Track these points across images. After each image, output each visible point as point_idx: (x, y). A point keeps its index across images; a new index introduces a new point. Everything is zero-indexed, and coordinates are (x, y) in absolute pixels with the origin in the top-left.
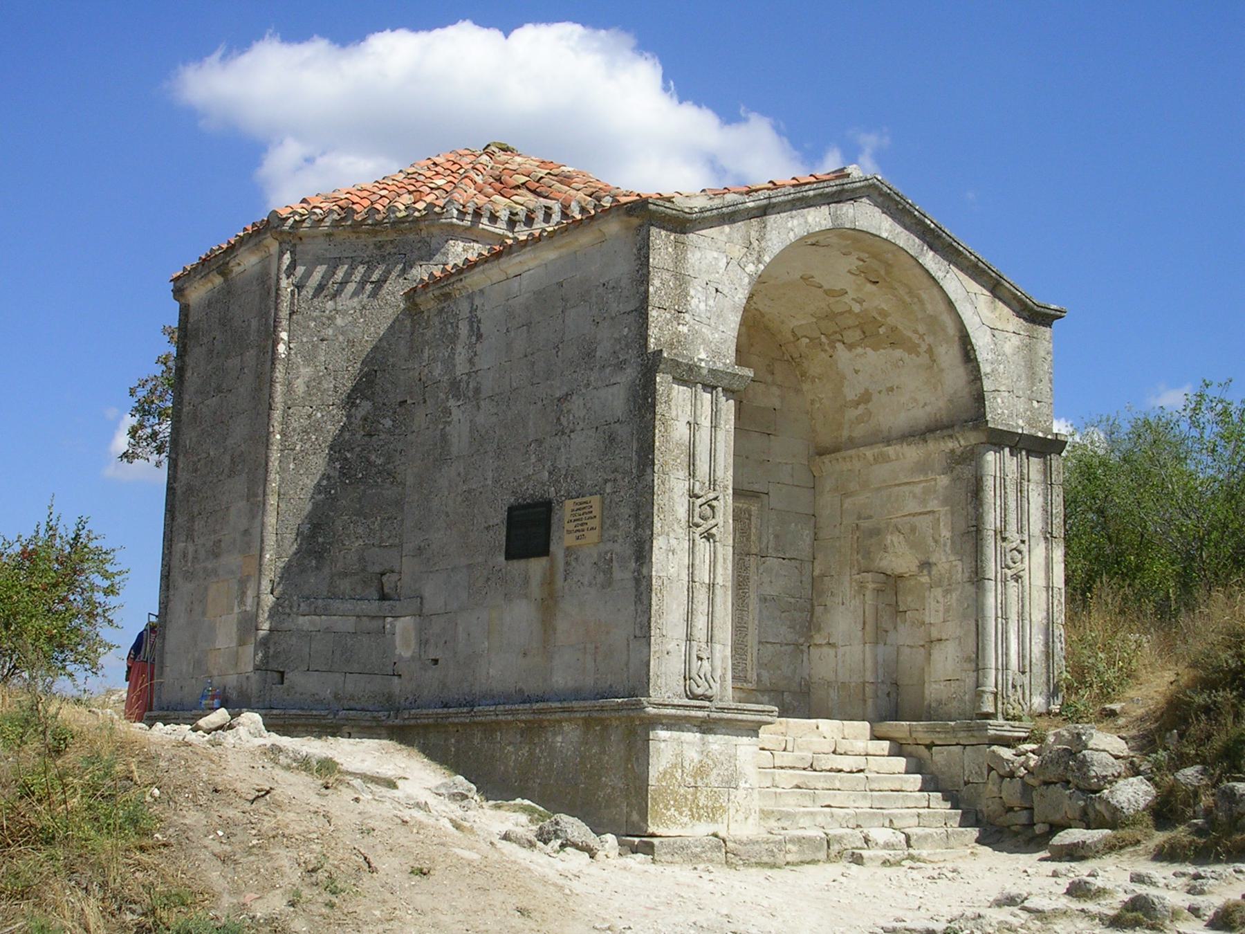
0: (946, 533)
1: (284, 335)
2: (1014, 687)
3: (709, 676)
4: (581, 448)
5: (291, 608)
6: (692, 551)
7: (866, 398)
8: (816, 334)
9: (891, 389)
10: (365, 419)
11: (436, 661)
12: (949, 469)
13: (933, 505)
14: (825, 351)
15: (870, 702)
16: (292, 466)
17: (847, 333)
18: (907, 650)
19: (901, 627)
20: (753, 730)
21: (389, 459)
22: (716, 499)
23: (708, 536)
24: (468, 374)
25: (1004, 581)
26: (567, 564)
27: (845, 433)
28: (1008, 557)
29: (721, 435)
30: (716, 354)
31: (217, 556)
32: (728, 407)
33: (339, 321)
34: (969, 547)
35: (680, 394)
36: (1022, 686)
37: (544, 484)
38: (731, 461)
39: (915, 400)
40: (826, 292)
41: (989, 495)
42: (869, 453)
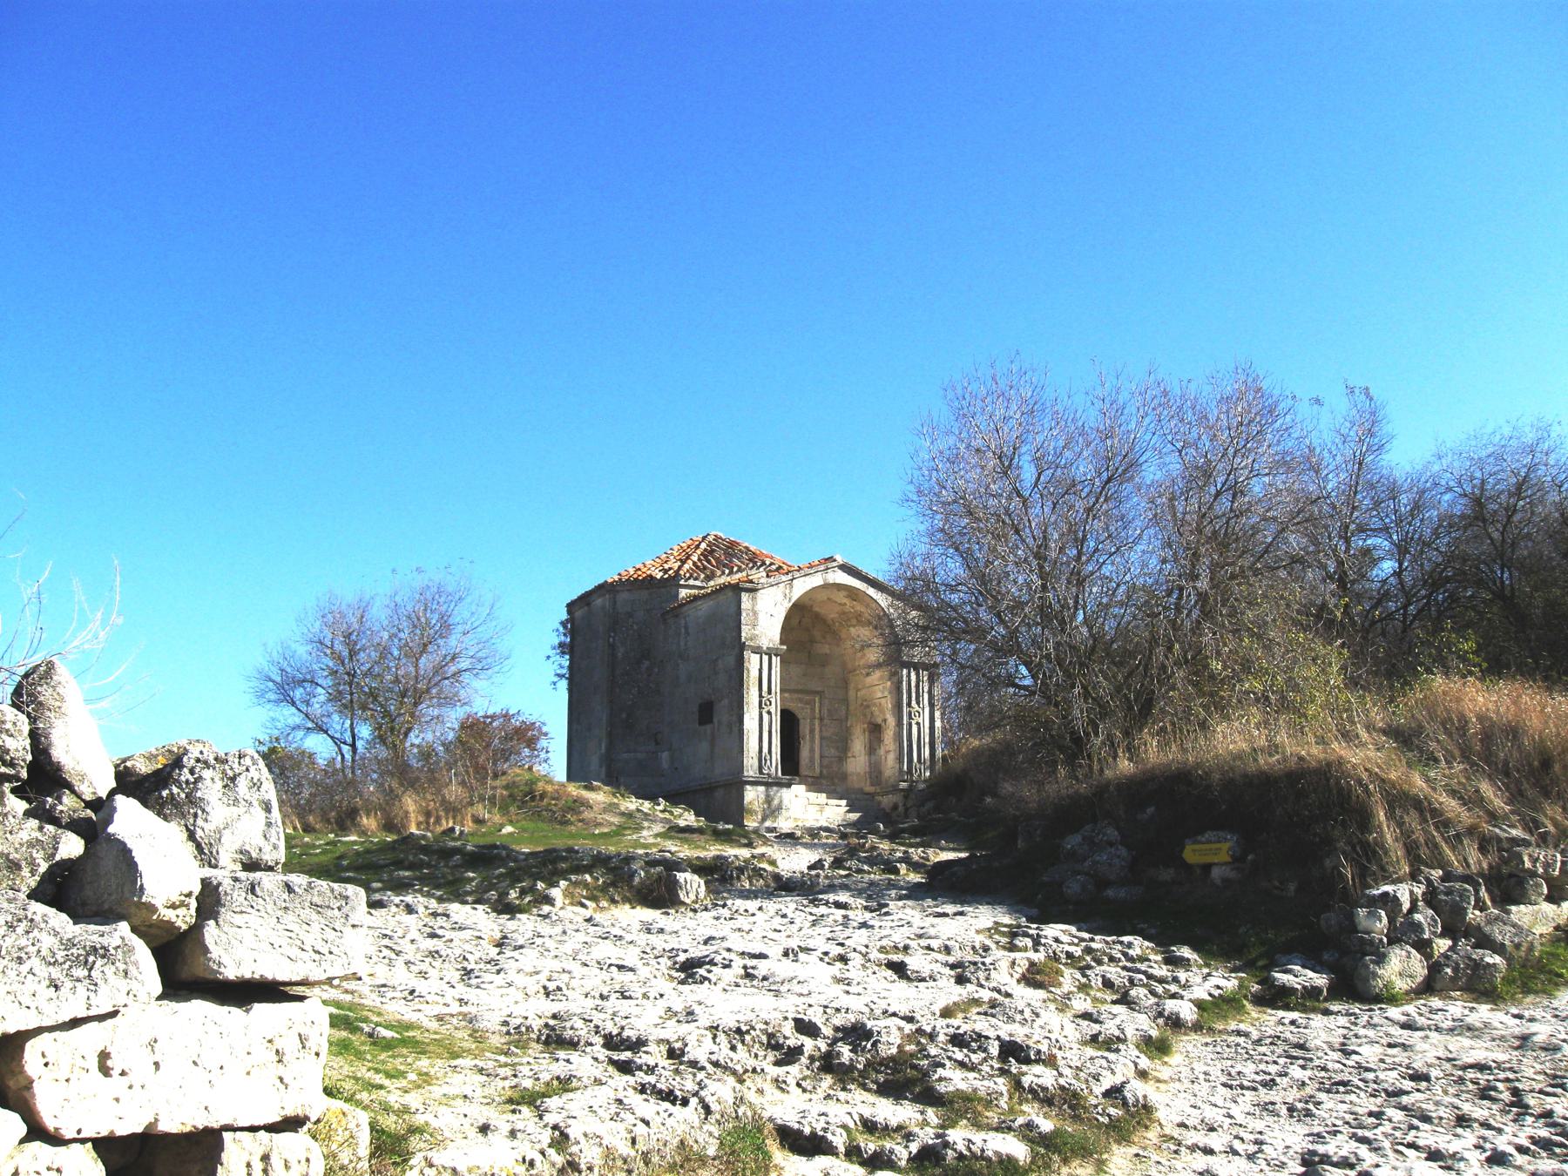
20: (789, 785)
35: (755, 658)
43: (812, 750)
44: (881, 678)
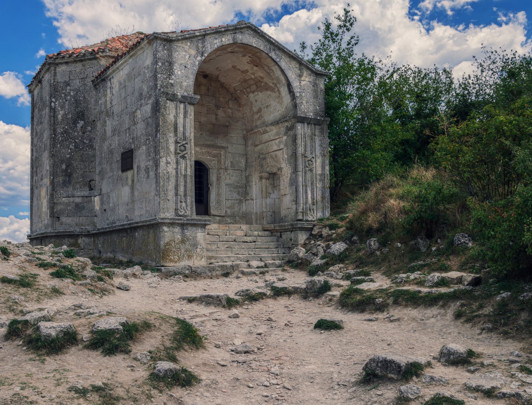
0: (286, 156)
1: (53, 100)
2: (310, 210)
3: (185, 208)
4: (140, 129)
5: (60, 195)
6: (177, 163)
7: (260, 110)
8: (242, 89)
9: (267, 107)
10: (82, 127)
11: (105, 210)
12: (286, 134)
13: (282, 146)
14: (245, 94)
15: (265, 219)
16: (59, 146)
17: (252, 87)
18: (277, 200)
19: (276, 192)
21: (90, 141)
22: (187, 143)
23: (183, 157)
24: (110, 108)
25: (305, 173)
26: (138, 171)
27: (254, 124)
28: (307, 163)
29: (187, 120)
30: (186, 91)
31: (42, 179)
32: (191, 109)
33: (72, 94)
34: (292, 160)
35: (171, 105)
36: (313, 210)
37: (130, 143)
38: (193, 130)
39: (276, 110)
40: (242, 72)
41: (299, 141)
42: (261, 130)
43: (218, 195)
44: (277, 134)
